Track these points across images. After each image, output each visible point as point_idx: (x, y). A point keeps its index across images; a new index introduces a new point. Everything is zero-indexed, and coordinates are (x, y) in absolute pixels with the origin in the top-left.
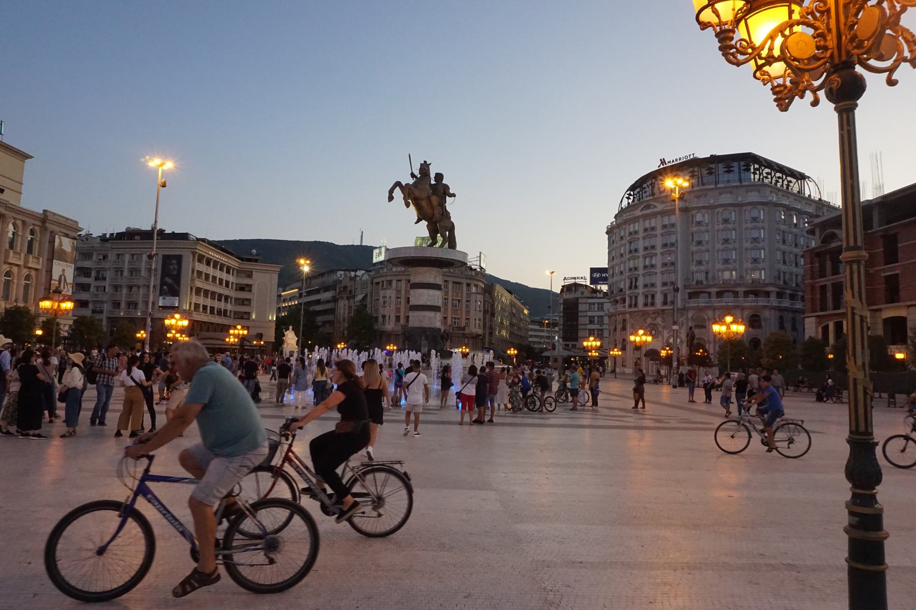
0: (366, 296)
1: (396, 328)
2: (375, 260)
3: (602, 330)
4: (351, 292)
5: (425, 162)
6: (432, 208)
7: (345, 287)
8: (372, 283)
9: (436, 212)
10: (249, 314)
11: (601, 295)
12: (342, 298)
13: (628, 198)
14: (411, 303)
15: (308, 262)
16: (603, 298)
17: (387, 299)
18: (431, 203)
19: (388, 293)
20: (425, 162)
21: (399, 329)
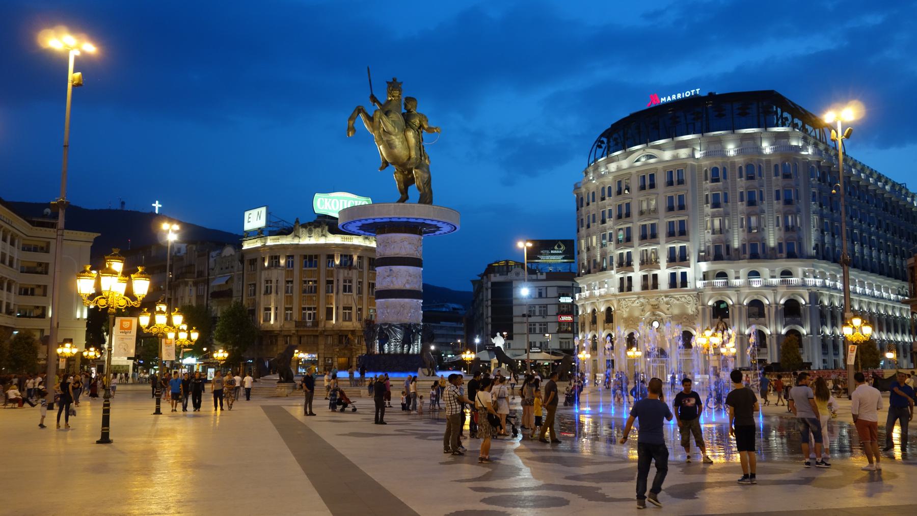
0: (231, 278)
1: (287, 326)
2: (248, 226)
3: (546, 324)
4: (200, 274)
5: (394, 80)
6: (409, 148)
7: (191, 265)
8: (242, 261)
9: (413, 154)
10: (44, 310)
11: (544, 277)
12: (186, 284)
13: (600, 147)
14: (378, 287)
15: (176, 227)
16: (548, 279)
17: (274, 285)
18: (407, 140)
19: (275, 274)
20: (394, 80)
21: (291, 327)
